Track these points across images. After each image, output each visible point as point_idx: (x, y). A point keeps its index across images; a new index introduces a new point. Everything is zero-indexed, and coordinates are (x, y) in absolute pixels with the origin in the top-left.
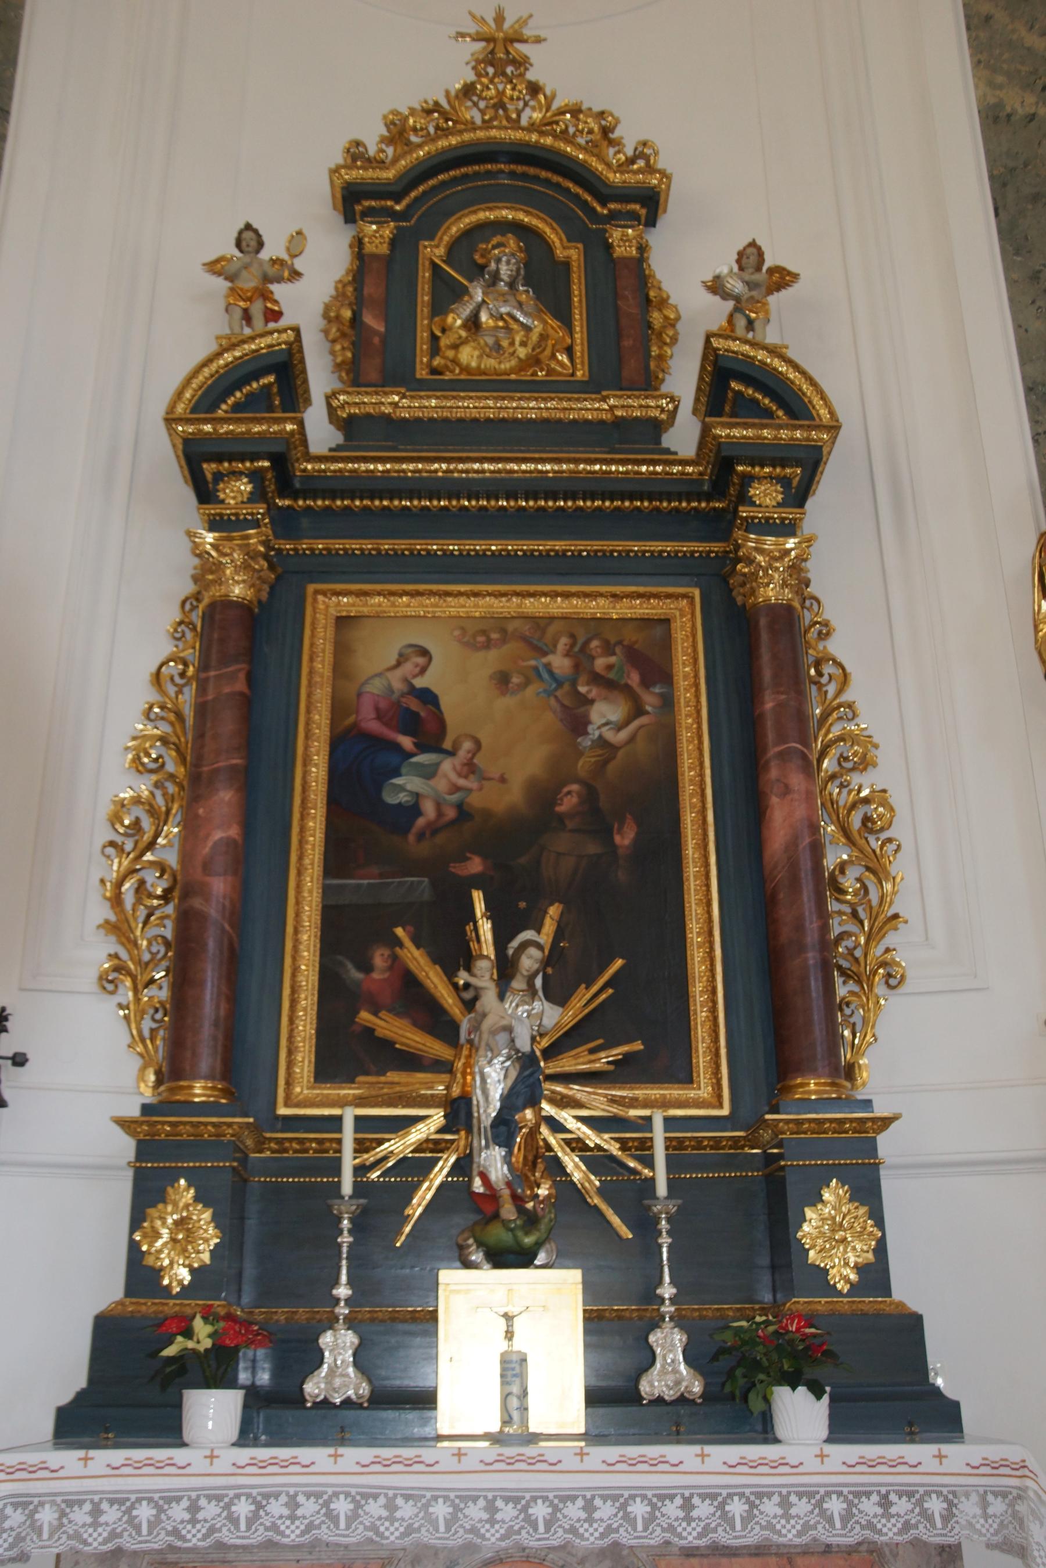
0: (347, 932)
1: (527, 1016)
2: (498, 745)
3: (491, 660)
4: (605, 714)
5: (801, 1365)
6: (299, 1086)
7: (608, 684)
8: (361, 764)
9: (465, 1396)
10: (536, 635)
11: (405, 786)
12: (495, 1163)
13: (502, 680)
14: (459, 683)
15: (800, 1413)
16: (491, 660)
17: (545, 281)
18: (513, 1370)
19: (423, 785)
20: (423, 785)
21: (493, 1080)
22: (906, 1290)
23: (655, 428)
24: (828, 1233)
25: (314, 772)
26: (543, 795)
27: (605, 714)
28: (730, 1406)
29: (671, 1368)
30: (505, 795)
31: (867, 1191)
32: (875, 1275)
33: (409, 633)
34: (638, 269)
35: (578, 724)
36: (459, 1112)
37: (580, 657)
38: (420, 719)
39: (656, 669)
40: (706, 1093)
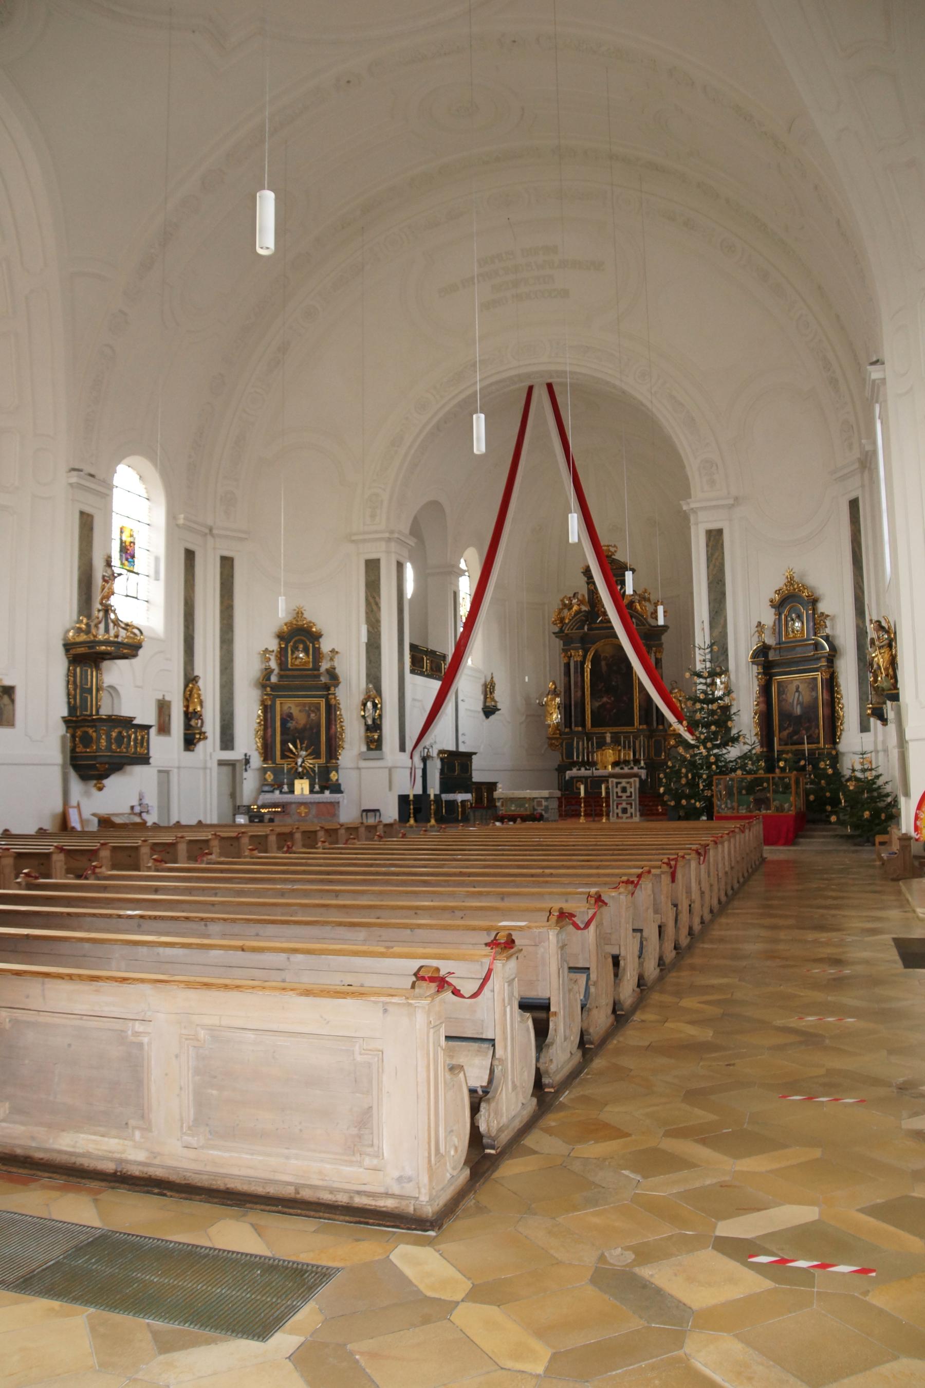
0: (284, 743)
1: (304, 753)
2: (300, 719)
3: (299, 708)
4: (313, 715)
5: (327, 788)
6: (278, 759)
7: (313, 711)
8: (284, 722)
9: (297, 791)
10: (304, 705)
11: (289, 725)
12: (300, 769)
13: (300, 711)
14: (295, 711)
15: (327, 792)
16: (299, 708)
17: (306, 650)
18: (302, 789)
19: (291, 725)
20: (291, 725)
21: (300, 761)
22: (340, 781)
23: (318, 676)
24: (333, 776)
25: (278, 724)
26: (305, 725)
27: (313, 715)
28: (322, 792)
29: (317, 788)
30: (300, 726)
31: (337, 772)
32: (337, 780)
33: (289, 705)
34: (319, 648)
35: (309, 716)
36: (296, 764)
37: (310, 708)
38: (290, 716)
39: (318, 709)
40: (323, 761)
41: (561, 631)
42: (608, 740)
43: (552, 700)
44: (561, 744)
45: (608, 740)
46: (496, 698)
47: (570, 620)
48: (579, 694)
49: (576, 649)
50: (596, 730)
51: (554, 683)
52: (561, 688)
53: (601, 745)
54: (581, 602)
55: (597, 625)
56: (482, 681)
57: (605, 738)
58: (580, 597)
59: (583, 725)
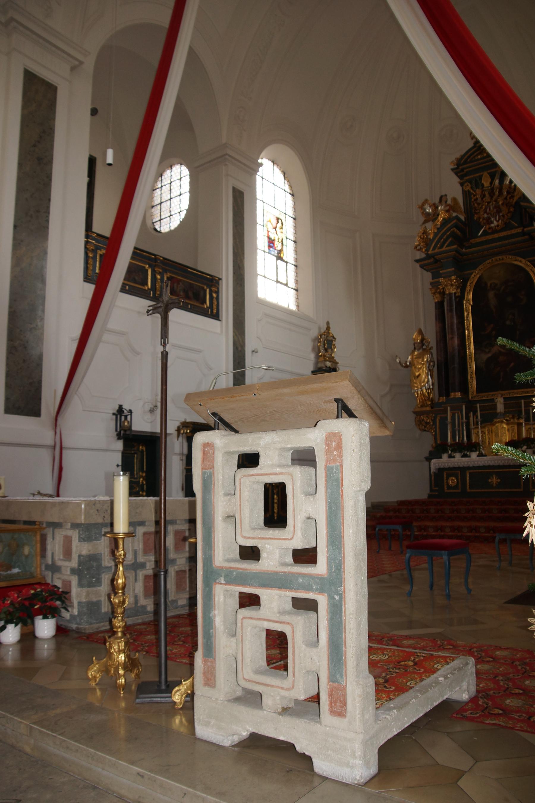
41: (428, 257)
42: (500, 408)
43: (418, 357)
44: (434, 421)
45: (500, 408)
46: (337, 359)
47: (436, 235)
48: (456, 342)
49: (447, 276)
50: (485, 396)
51: (420, 332)
52: (431, 337)
53: (489, 417)
54: (451, 209)
55: (478, 240)
56: (315, 333)
57: (495, 407)
58: (449, 202)
59: (465, 389)
